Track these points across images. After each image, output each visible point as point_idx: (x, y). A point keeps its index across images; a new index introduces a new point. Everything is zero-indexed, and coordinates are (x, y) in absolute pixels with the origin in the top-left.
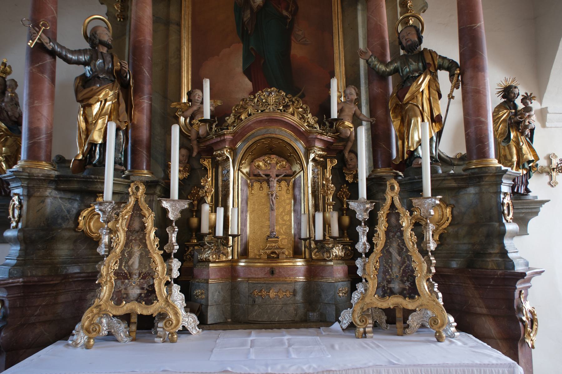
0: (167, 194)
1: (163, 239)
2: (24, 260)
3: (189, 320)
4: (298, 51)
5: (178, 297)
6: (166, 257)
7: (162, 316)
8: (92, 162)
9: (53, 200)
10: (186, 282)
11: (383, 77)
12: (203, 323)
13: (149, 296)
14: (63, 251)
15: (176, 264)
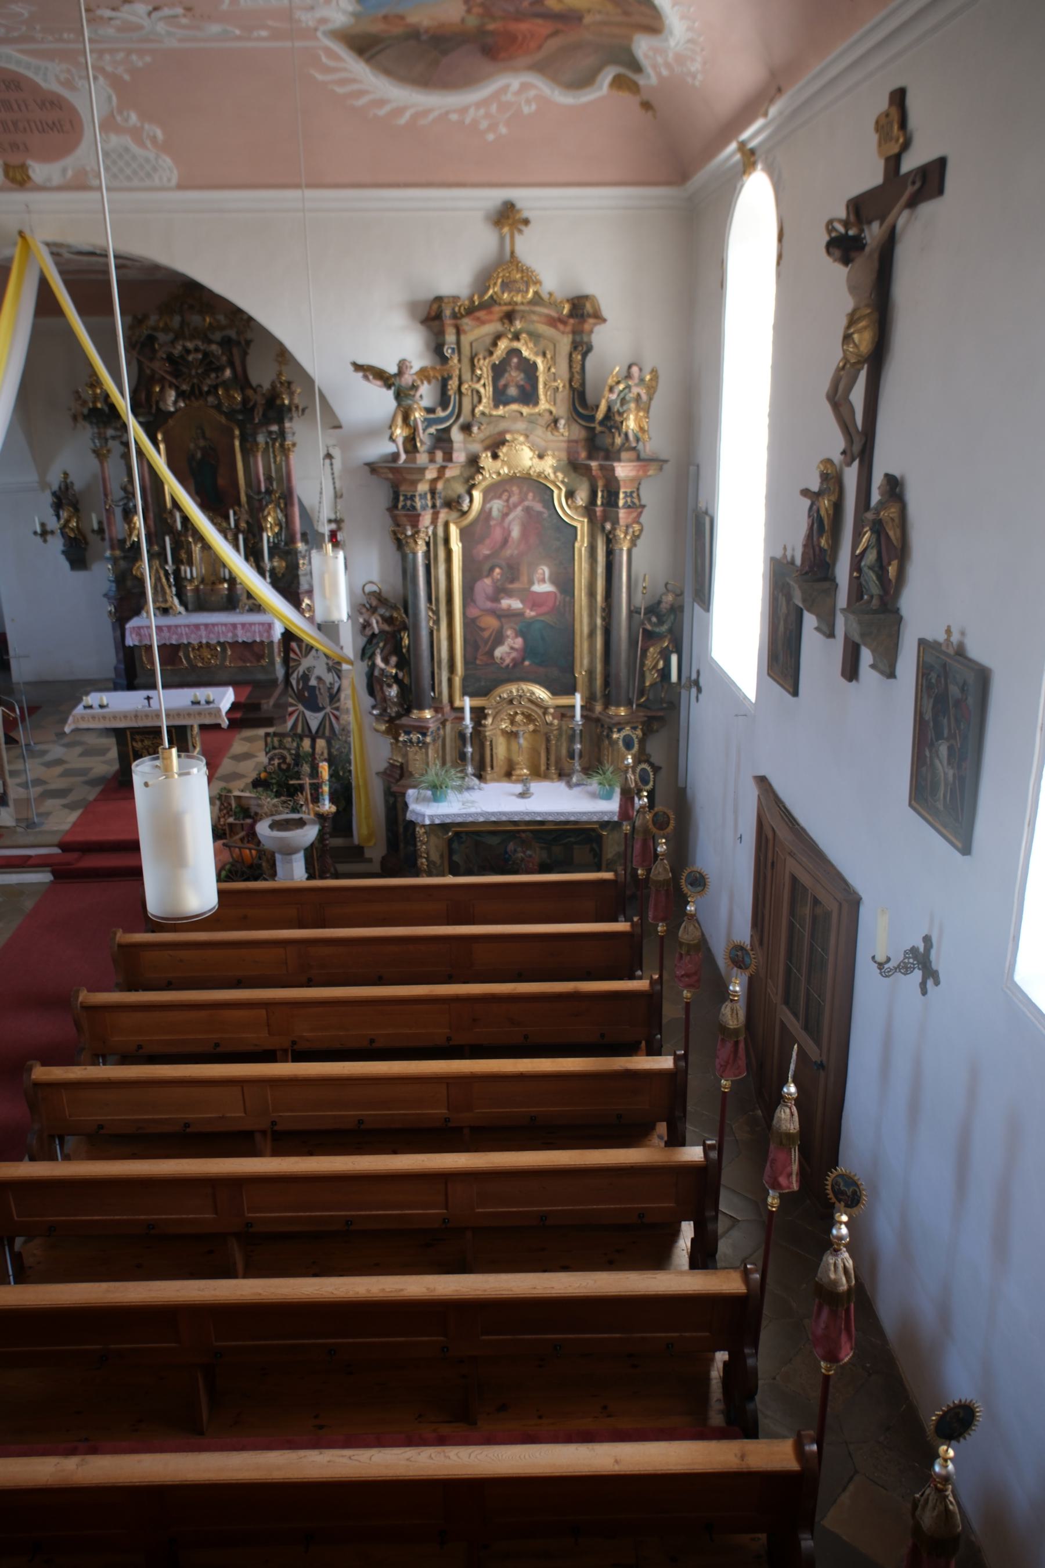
0: (166, 562)
1: (168, 580)
2: (118, 587)
3: (181, 609)
4: (221, 482)
5: (176, 601)
6: (170, 587)
7: (171, 607)
8: (136, 547)
9: (122, 564)
10: (180, 595)
11: (260, 501)
12: (187, 609)
13: (166, 601)
14: (129, 583)
15: (174, 589)
